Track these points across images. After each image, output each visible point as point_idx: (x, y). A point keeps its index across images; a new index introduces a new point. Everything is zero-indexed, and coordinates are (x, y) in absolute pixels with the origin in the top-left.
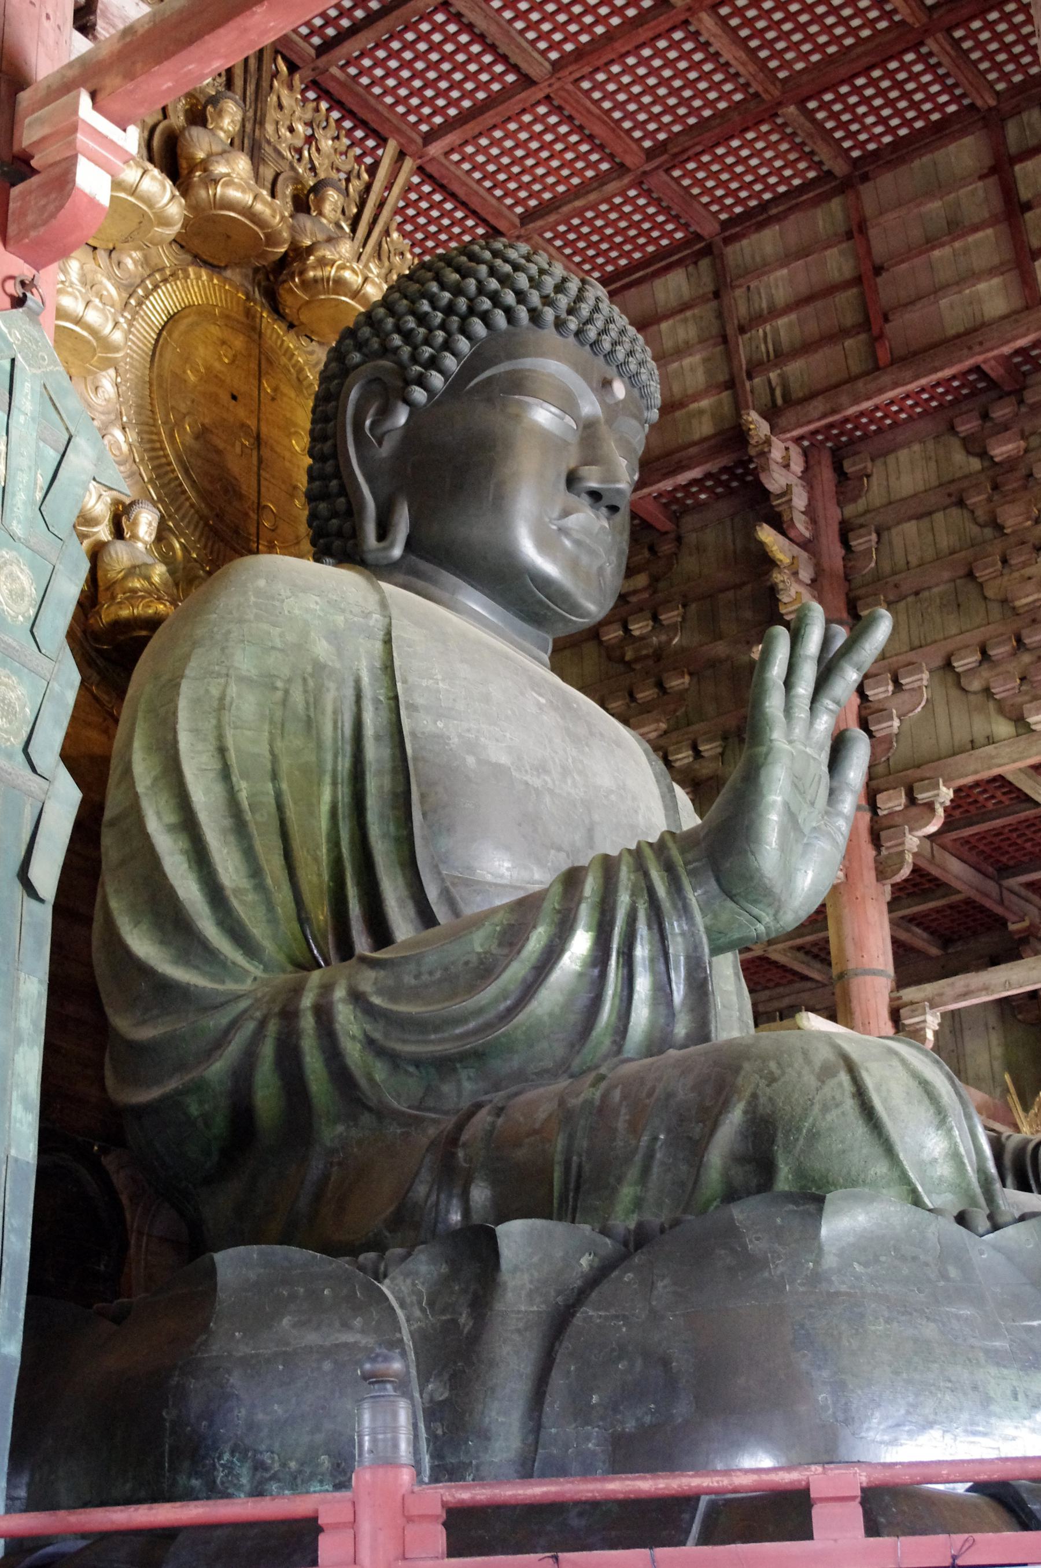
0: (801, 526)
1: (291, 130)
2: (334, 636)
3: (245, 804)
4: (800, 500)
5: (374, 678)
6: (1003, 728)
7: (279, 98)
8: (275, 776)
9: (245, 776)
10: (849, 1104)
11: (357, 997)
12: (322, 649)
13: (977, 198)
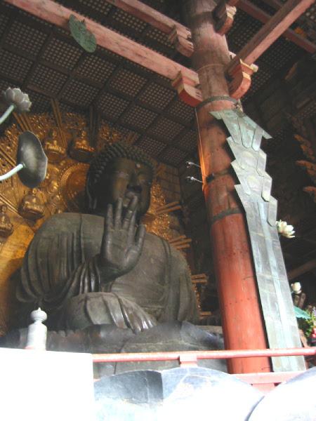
3: (39, 263)
5: (77, 233)
10: (82, 309)
11: (43, 300)
12: (64, 229)
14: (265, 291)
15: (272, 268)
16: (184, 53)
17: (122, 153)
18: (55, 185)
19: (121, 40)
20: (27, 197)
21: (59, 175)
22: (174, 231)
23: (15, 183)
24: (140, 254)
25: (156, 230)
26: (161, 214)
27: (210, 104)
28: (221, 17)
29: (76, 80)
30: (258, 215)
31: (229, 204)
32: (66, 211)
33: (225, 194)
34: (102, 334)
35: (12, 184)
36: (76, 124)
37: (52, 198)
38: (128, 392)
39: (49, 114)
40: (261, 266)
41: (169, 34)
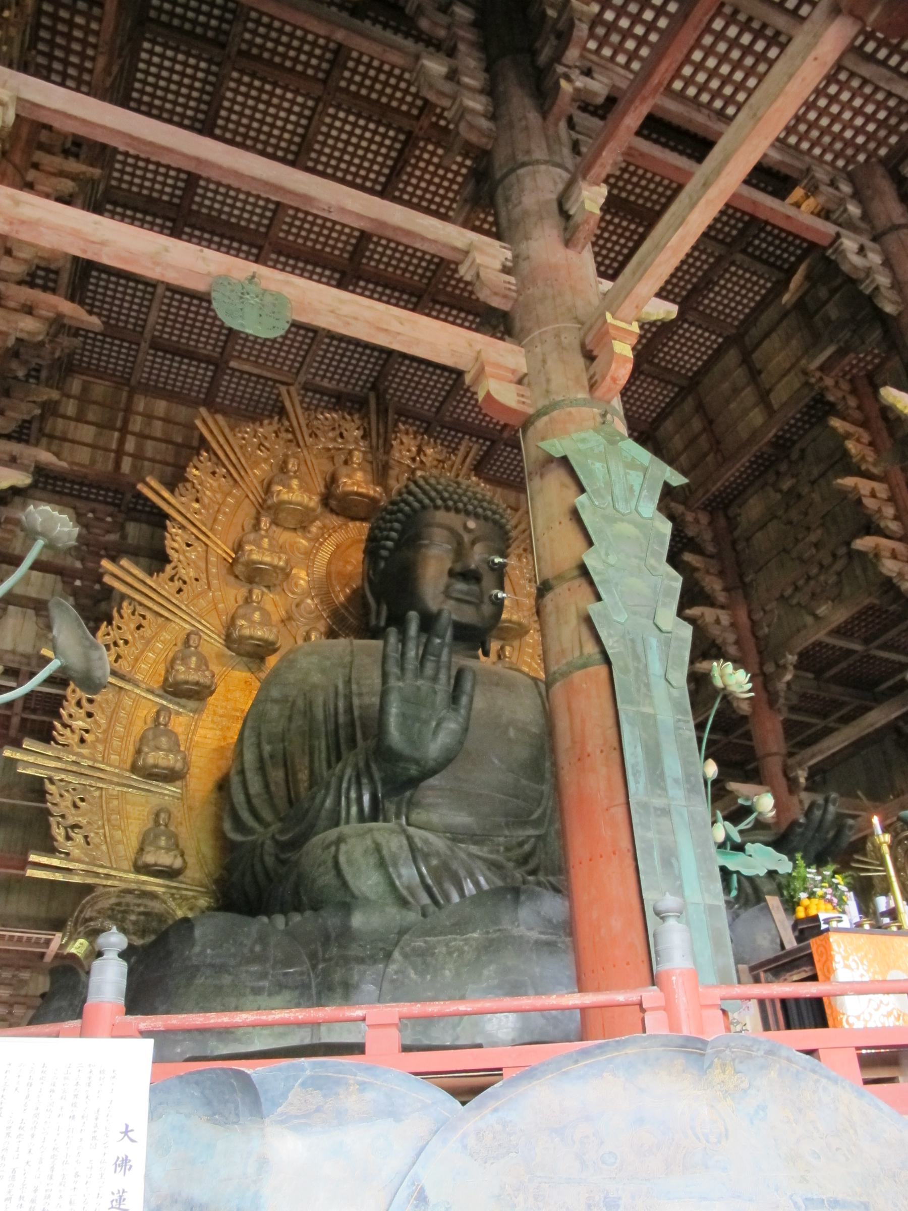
0: (711, 548)
2: (323, 671)
3: (266, 755)
4: (708, 536)
6: (809, 620)
8: (283, 740)
9: (269, 743)
10: (330, 863)
11: (273, 837)
12: (316, 678)
13: (740, 375)
14: (650, 835)
15: (669, 781)
16: (496, 302)
17: (432, 500)
18: (301, 576)
19: (342, 301)
20: (241, 611)
21: (309, 555)
23: (215, 582)
24: (466, 730)
25: (532, 657)
27: (545, 419)
28: (572, 212)
30: (641, 667)
31: (581, 647)
32: (331, 634)
33: (573, 620)
34: (357, 920)
35: (209, 584)
36: (341, 436)
37: (298, 605)
38: (209, 1103)
39: (280, 420)
40: (642, 779)
41: (462, 262)
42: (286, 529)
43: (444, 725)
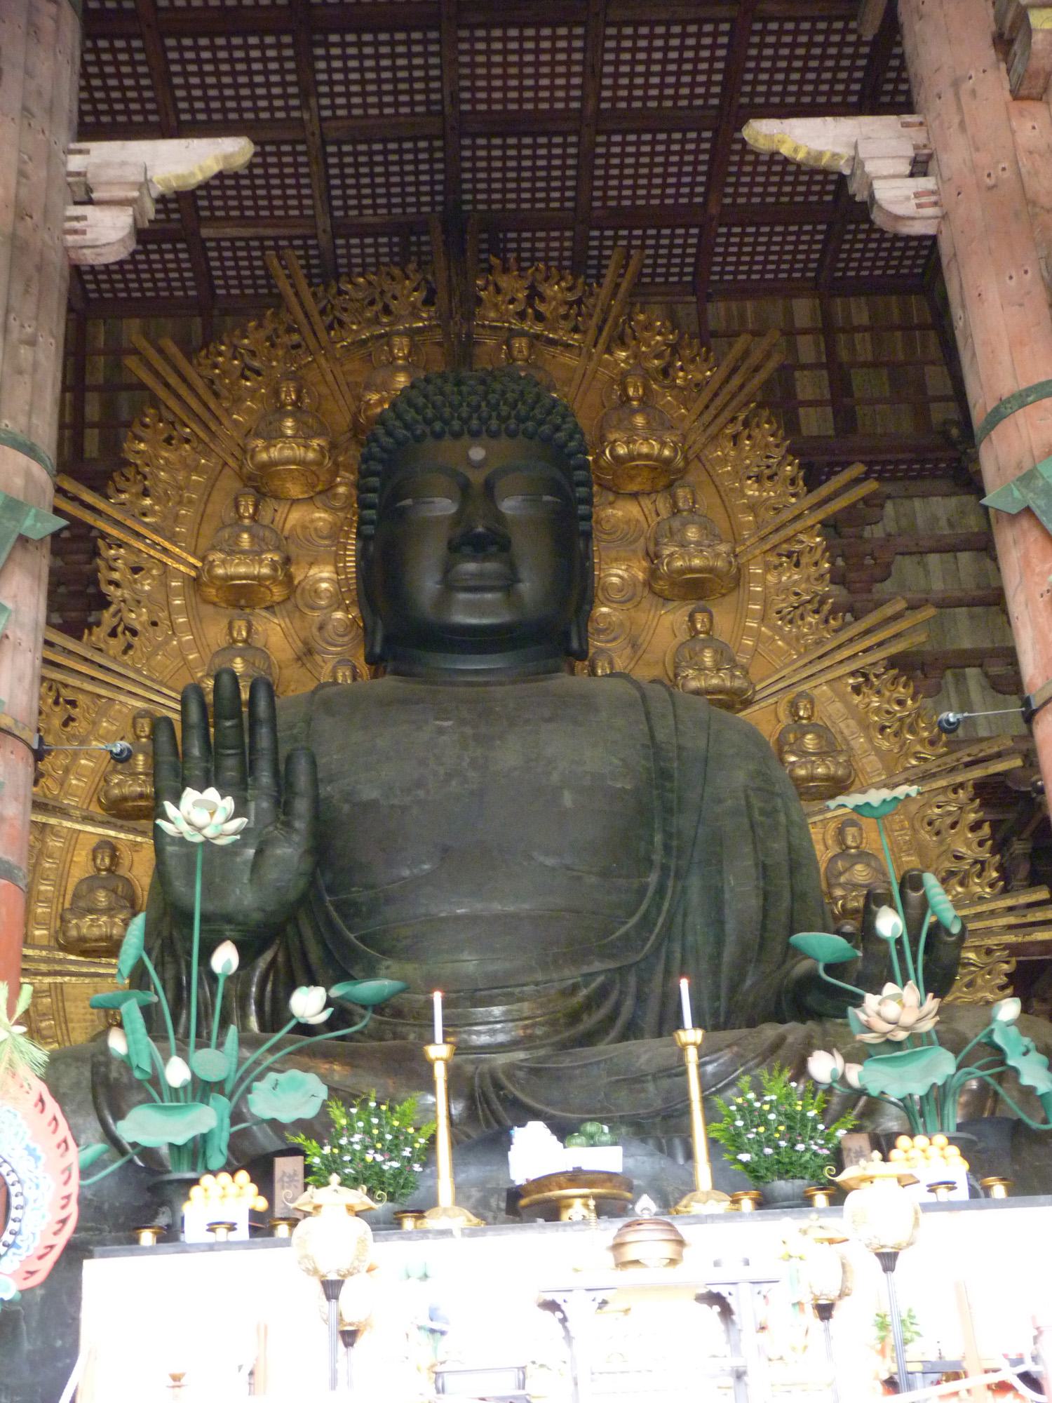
1: (512, 301)
7: (496, 285)
22: (965, 557)
26: (787, 540)
29: (339, 143)
36: (387, 310)
37: (321, 628)
39: (275, 315)
42: (295, 502)
43: (268, 853)
